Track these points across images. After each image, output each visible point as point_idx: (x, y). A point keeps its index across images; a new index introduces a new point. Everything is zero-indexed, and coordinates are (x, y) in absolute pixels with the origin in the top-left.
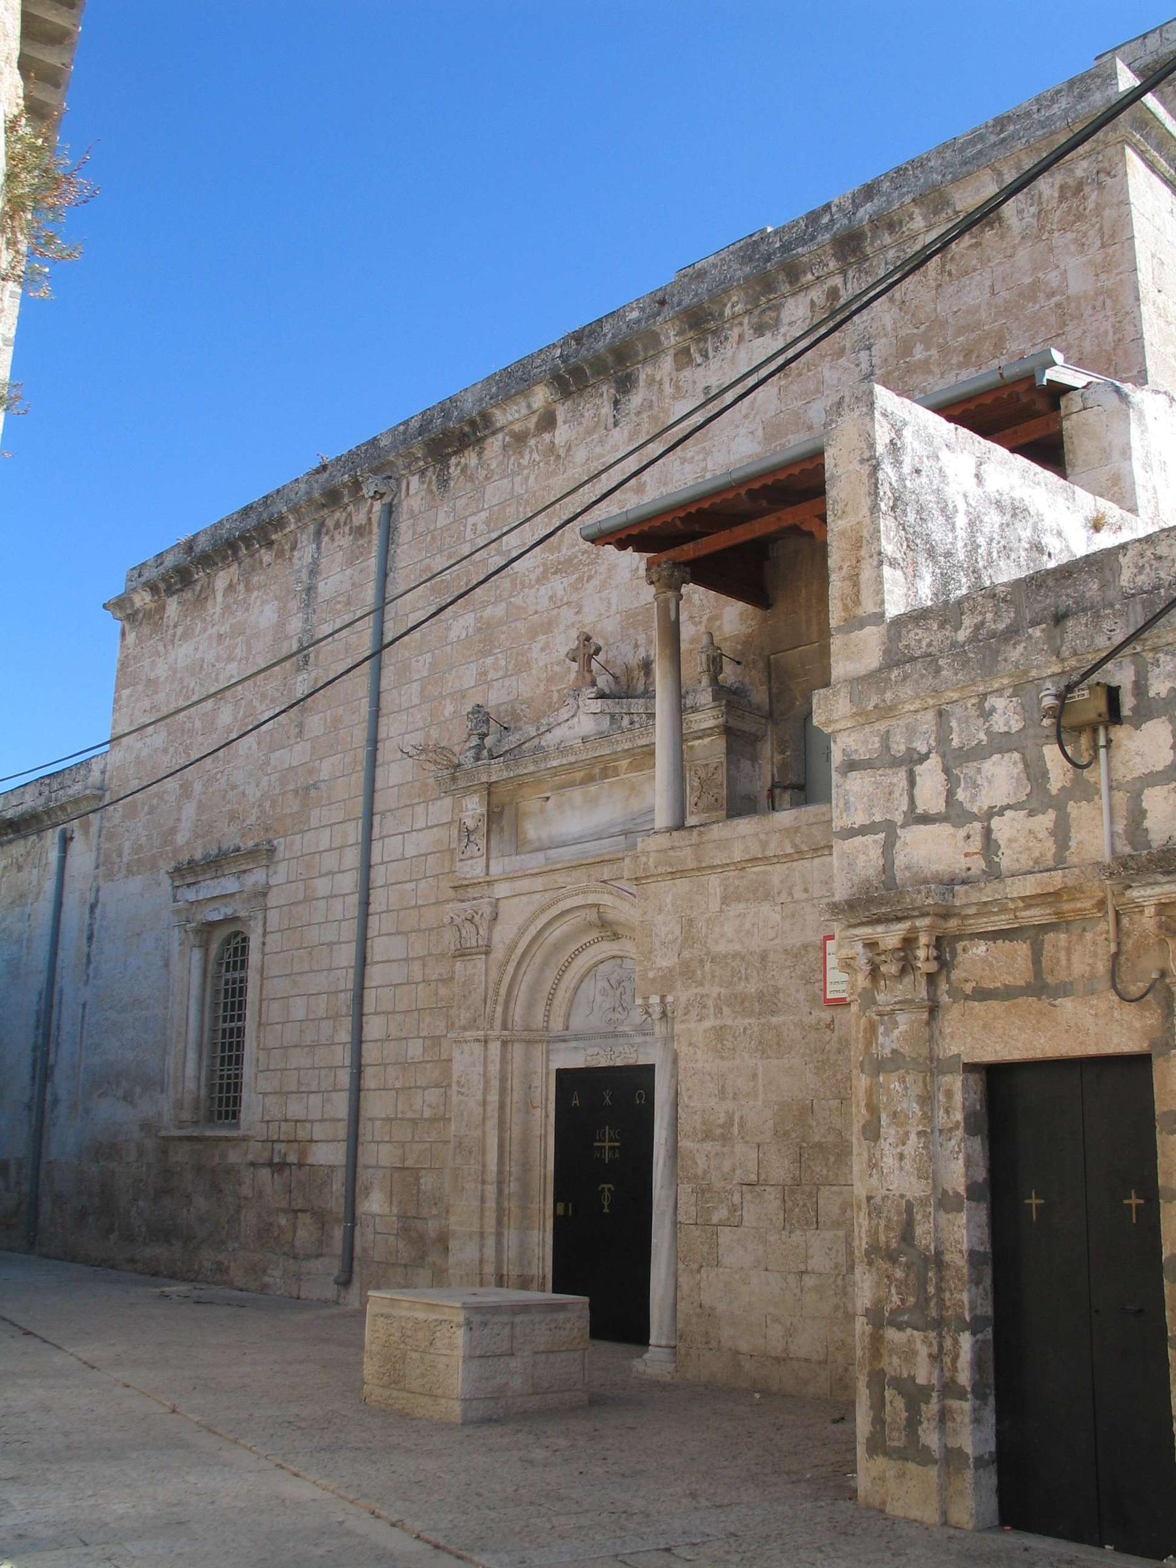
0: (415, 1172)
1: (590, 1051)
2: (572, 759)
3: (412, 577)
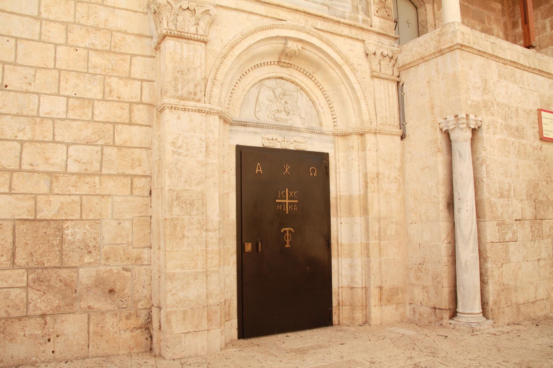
0: (58, 225)
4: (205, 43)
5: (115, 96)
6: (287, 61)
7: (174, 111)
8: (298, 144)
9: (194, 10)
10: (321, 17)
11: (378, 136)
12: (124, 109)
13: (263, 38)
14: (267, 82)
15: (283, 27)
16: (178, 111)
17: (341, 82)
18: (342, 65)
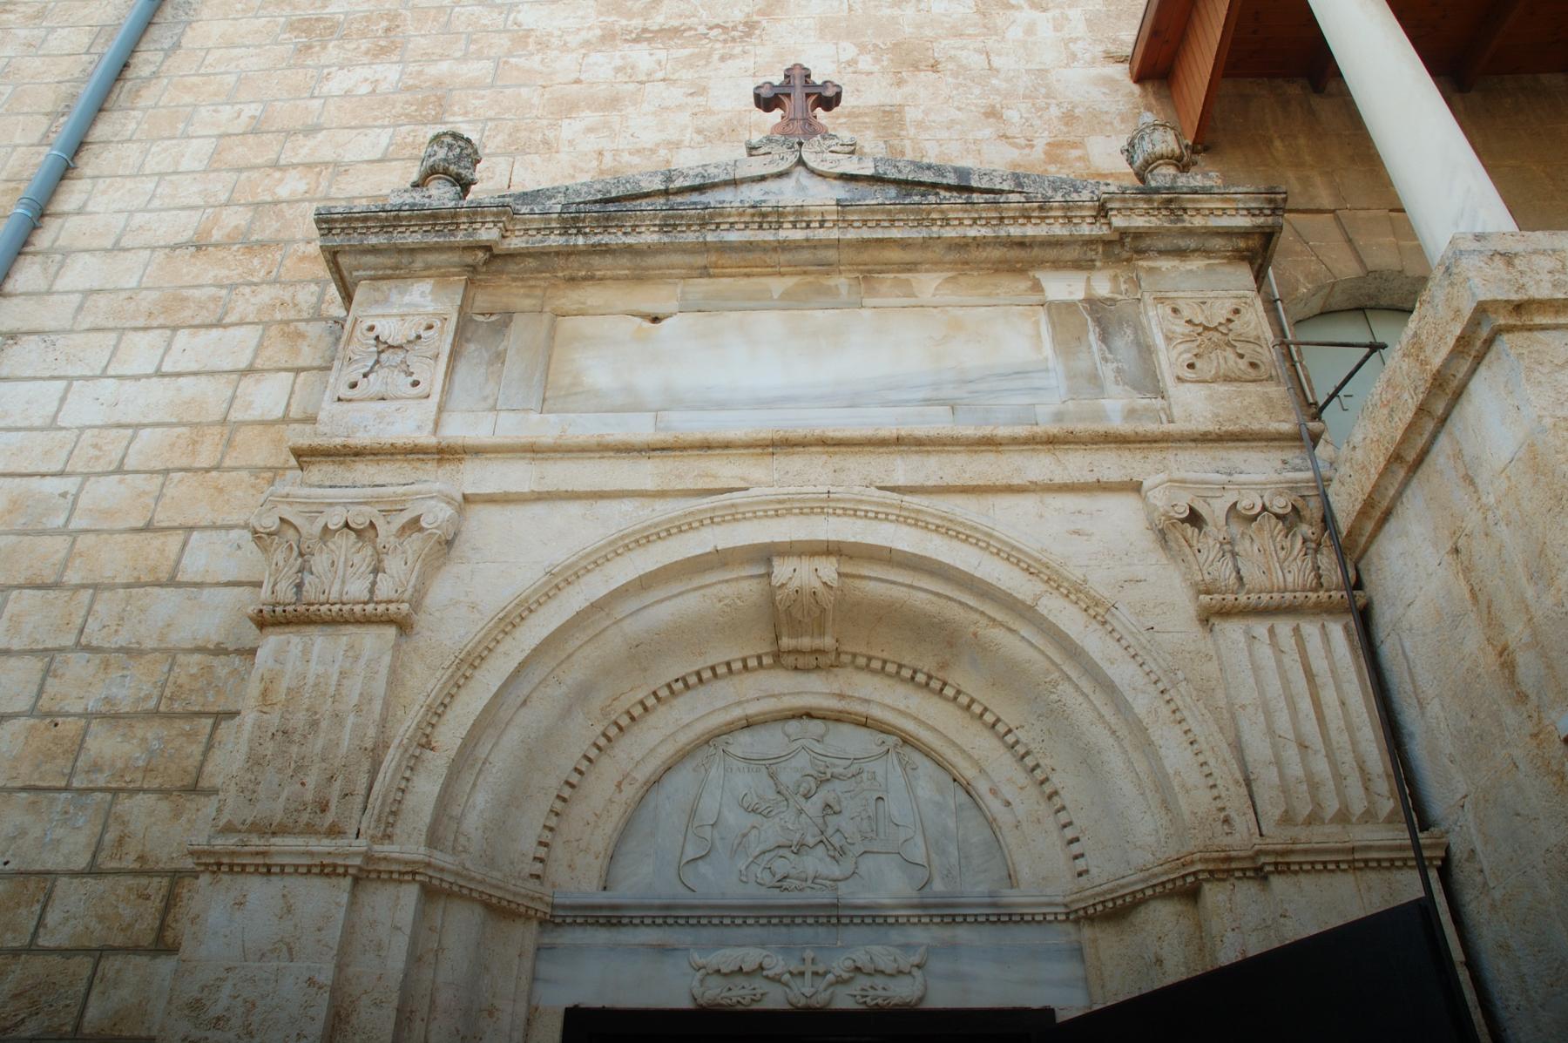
1: (727, 958)
2: (799, 235)
3: (239, 6)
4: (403, 625)
5: (133, 856)
6: (806, 642)
7: (226, 878)
8: (879, 981)
9: (372, 524)
10: (899, 441)
11: (1277, 882)
12: (148, 898)
13: (651, 567)
14: (743, 743)
15: (735, 516)
16: (240, 879)
17: (1056, 675)
18: (1038, 598)
